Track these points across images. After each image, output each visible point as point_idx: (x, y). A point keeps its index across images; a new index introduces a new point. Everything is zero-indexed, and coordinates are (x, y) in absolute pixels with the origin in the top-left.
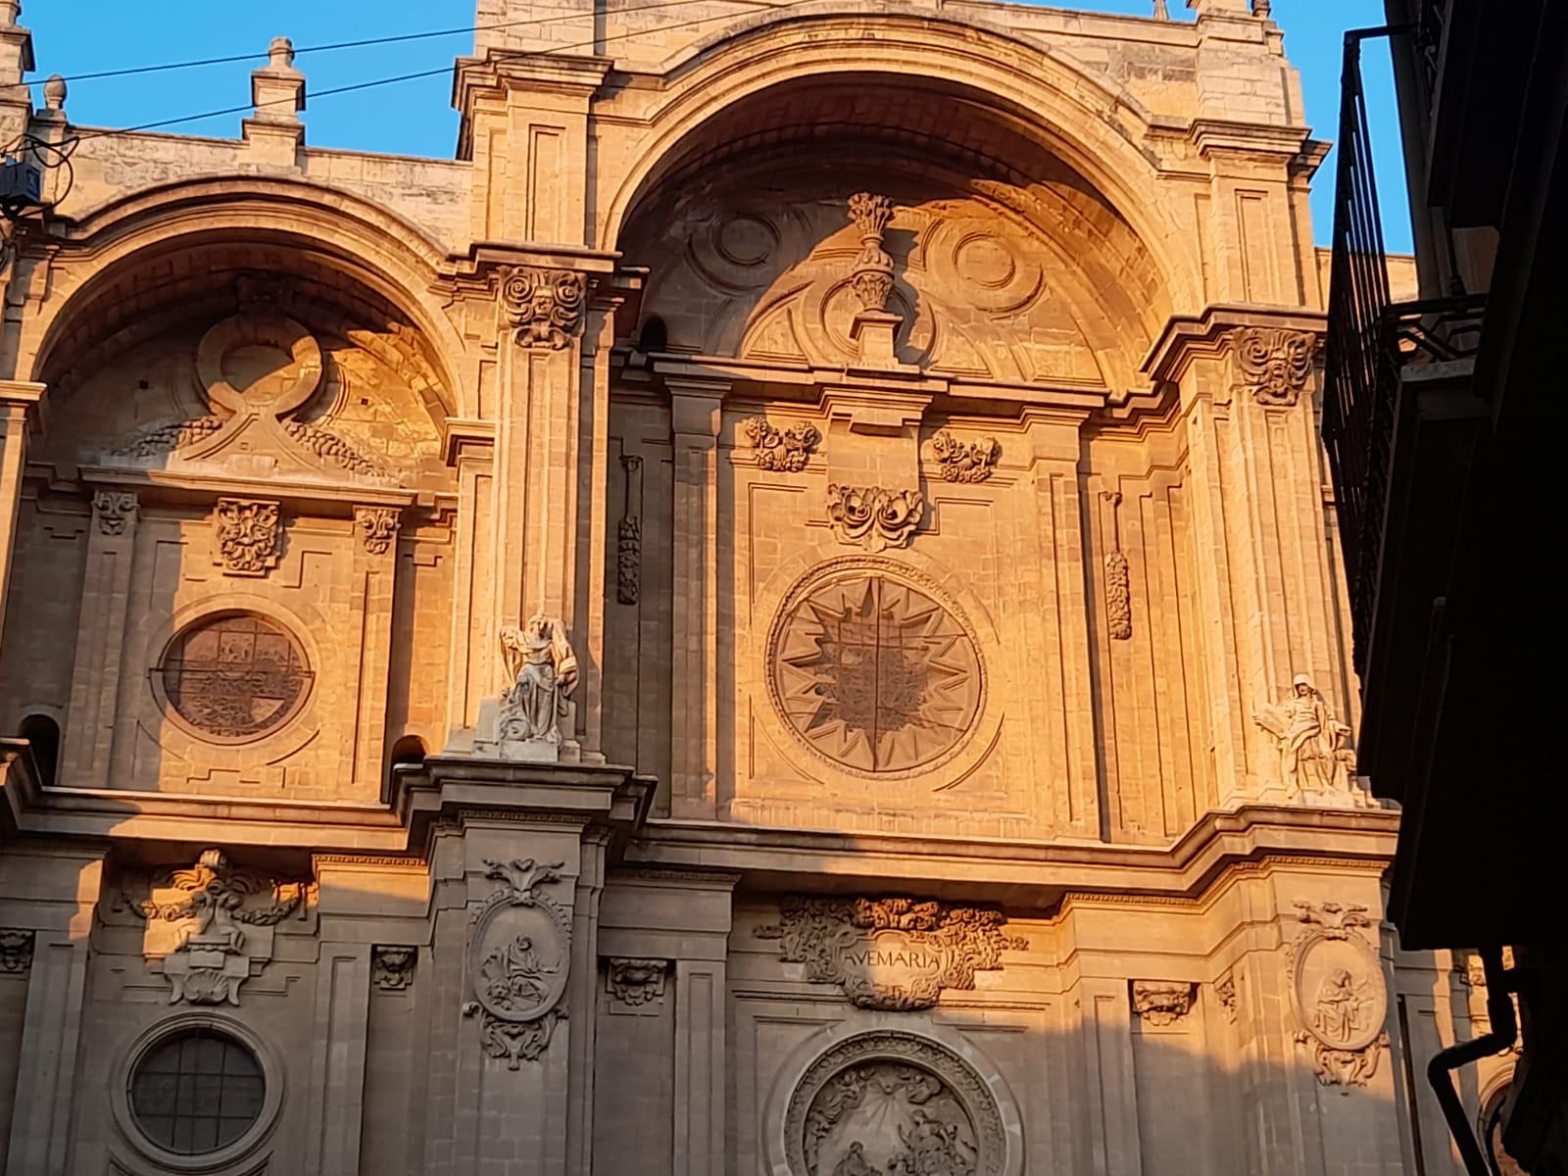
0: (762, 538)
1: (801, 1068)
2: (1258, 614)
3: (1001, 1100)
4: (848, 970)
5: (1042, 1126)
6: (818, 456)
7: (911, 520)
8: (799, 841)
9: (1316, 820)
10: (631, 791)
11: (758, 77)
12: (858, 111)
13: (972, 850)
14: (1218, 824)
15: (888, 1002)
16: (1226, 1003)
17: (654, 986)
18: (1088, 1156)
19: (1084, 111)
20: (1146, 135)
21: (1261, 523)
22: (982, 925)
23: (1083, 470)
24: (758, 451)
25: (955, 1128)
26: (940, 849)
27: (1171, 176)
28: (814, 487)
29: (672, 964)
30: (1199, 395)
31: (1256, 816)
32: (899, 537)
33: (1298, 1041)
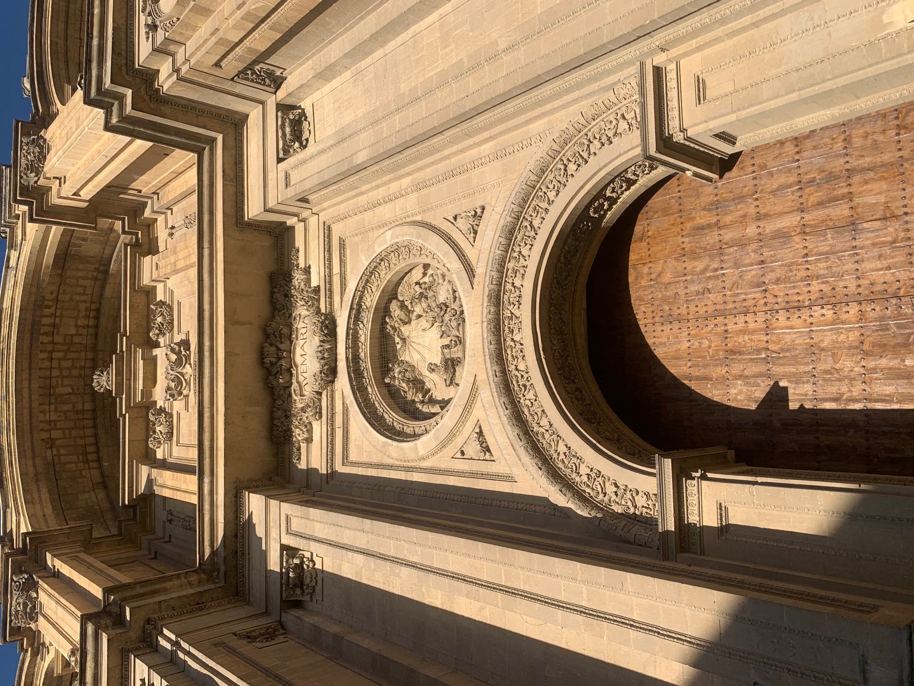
0: (192, 438)
1: (365, 426)
2: (86, 129)
3: (375, 252)
4: (308, 391)
6: (166, 406)
7: (177, 349)
8: (207, 443)
10: (115, 609)
11: (15, 455)
12: (71, 391)
13: (206, 307)
14: (114, 120)
15: (326, 355)
17: (305, 560)
20: (15, 250)
21: (67, 141)
22: (286, 285)
24: (162, 442)
25: (417, 283)
28: (178, 406)
29: (284, 548)
30: (61, 197)
32: (184, 355)
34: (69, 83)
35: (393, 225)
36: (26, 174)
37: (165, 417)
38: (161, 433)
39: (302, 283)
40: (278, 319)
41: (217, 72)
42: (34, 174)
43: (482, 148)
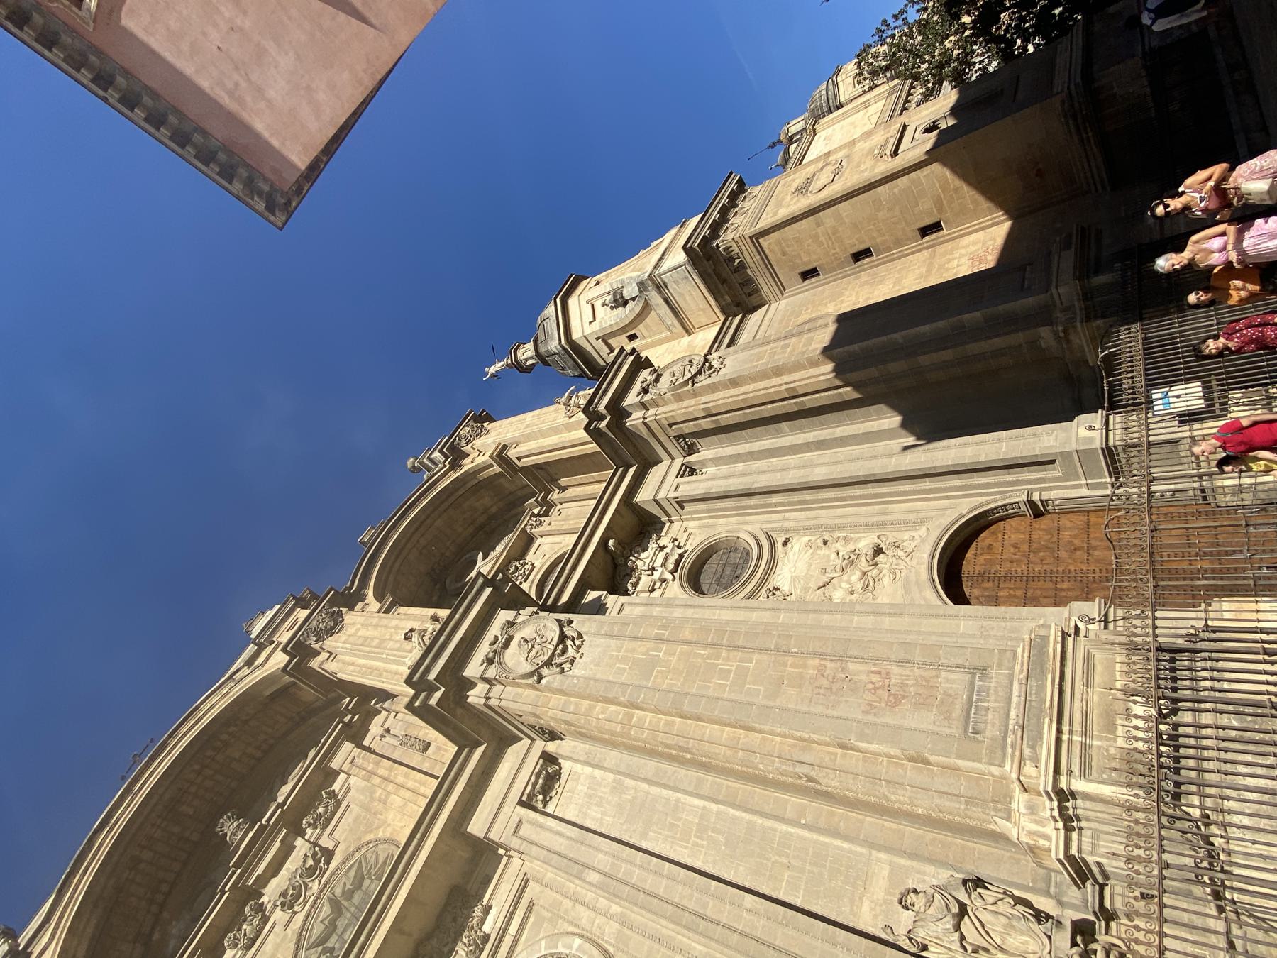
2: (384, 656)
5: (585, 915)
6: (269, 907)
9: (442, 639)
13: (384, 898)
16: (553, 736)
18: (590, 883)
19: (227, 694)
21: (361, 645)
23: (368, 749)
26: (369, 926)
27: (266, 660)
28: (279, 916)
31: (418, 675)
32: (321, 867)
33: (539, 682)
34: (393, 594)
35: (584, 933)
36: (307, 633)
37: (260, 920)
38: (245, 935)
39: (476, 920)
40: (434, 942)
41: (517, 717)
42: (315, 639)
43: (694, 944)
